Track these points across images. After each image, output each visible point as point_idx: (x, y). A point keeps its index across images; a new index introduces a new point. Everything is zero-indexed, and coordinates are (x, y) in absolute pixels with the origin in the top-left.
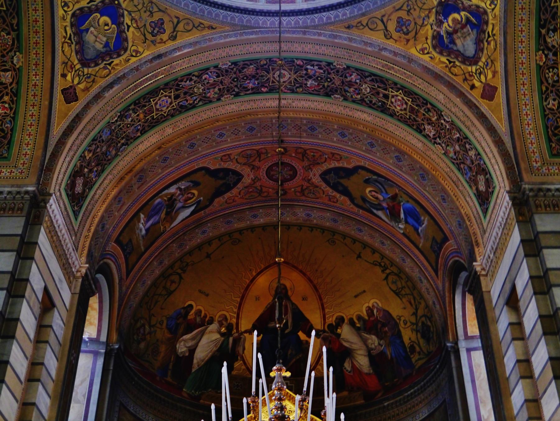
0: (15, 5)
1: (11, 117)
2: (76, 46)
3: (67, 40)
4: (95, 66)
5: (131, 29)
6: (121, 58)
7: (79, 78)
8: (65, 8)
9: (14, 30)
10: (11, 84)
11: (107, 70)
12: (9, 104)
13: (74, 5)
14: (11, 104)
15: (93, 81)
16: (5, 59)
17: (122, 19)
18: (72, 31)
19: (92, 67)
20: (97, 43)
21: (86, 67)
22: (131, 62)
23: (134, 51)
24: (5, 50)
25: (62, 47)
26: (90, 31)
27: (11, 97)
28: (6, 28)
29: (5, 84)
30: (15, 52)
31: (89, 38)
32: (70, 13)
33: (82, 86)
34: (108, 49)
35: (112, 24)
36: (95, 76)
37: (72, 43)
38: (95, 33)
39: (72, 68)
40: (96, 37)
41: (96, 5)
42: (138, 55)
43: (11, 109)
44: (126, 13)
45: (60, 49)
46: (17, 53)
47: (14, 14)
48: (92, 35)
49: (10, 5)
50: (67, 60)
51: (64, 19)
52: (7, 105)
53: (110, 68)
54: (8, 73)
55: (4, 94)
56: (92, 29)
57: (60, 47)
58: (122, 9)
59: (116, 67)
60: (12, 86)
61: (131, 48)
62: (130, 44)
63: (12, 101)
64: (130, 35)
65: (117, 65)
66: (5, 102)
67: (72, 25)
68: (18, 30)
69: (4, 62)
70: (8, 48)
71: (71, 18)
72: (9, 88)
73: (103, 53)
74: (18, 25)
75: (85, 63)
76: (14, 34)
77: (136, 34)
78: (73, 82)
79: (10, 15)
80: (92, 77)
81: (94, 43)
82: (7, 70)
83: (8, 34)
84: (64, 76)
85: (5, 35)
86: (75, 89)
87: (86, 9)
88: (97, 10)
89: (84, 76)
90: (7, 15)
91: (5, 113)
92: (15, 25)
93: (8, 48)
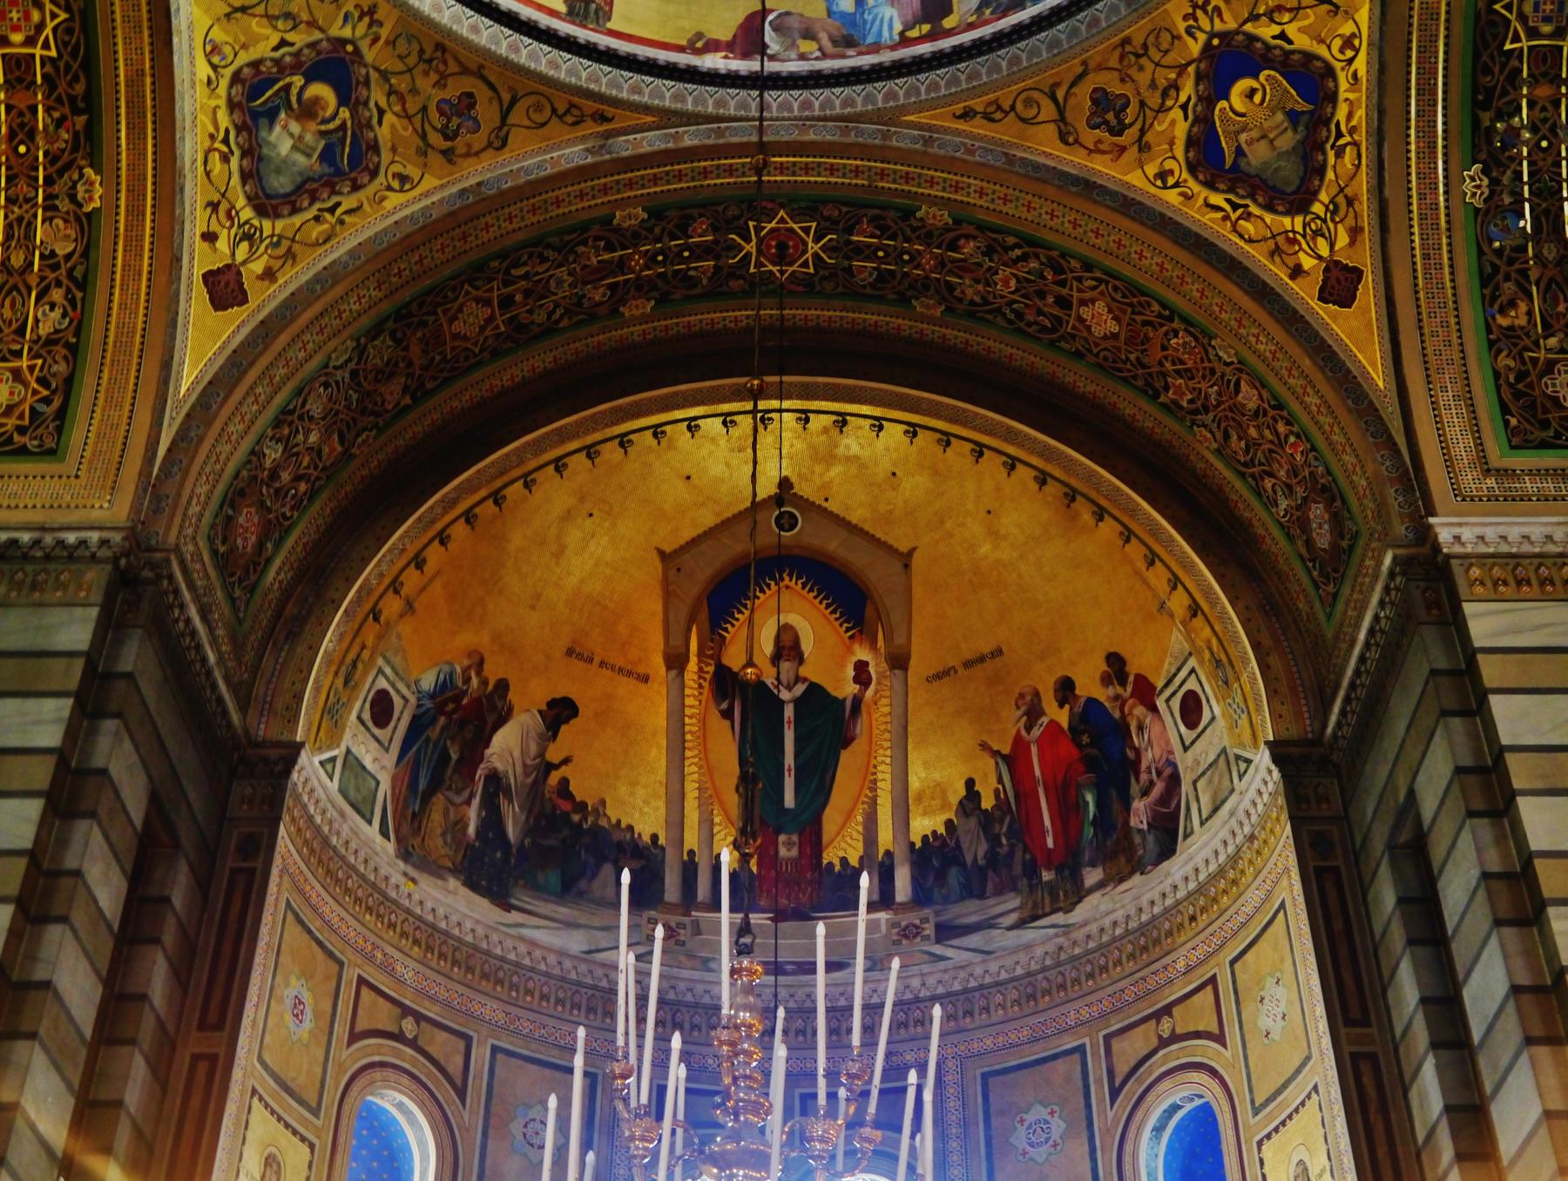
2: (1255, 201)
3: (1234, 217)
4: (1322, 180)
5: (1291, 31)
6: (1342, 95)
7: (1323, 235)
8: (1171, 181)
11: (1348, 149)
12: (1291, 432)
13: (1174, 158)
15: (1350, 202)
17: (1259, 45)
18: (1223, 192)
19: (1320, 187)
20: (1277, 143)
21: (1311, 203)
22: (1362, 73)
23: (1342, 51)
25: (1241, 237)
26: (1244, 146)
31: (1258, 155)
32: (1185, 175)
33: (1343, 240)
34: (1305, 119)
35: (1256, 77)
36: (1342, 190)
37: (1246, 206)
38: (1255, 134)
39: (1294, 241)
40: (1264, 137)
41: (1200, 99)
42: (1356, 42)
44: (1248, 27)
45: (1242, 243)
48: (1256, 145)
49: (1124, 296)
50: (1271, 244)
51: (1187, 197)
52: (1292, 439)
53: (1348, 139)
56: (1243, 137)
57: (1238, 241)
58: (1237, 32)
59: (1354, 123)
61: (1331, 53)
62: (1322, 51)
63: (1288, 423)
64: (1302, 42)
65: (1350, 116)
66: (1287, 437)
67: (1210, 185)
68: (1172, 312)
71: (1196, 178)
73: (1306, 137)
75: (1299, 202)
77: (1306, 23)
78: (1320, 257)
80: (1341, 199)
81: (1274, 148)
82: (1238, 384)
84: (1297, 272)
86: (1337, 263)
87: (1195, 130)
88: (1209, 101)
89: (1324, 221)
90: (1140, 313)
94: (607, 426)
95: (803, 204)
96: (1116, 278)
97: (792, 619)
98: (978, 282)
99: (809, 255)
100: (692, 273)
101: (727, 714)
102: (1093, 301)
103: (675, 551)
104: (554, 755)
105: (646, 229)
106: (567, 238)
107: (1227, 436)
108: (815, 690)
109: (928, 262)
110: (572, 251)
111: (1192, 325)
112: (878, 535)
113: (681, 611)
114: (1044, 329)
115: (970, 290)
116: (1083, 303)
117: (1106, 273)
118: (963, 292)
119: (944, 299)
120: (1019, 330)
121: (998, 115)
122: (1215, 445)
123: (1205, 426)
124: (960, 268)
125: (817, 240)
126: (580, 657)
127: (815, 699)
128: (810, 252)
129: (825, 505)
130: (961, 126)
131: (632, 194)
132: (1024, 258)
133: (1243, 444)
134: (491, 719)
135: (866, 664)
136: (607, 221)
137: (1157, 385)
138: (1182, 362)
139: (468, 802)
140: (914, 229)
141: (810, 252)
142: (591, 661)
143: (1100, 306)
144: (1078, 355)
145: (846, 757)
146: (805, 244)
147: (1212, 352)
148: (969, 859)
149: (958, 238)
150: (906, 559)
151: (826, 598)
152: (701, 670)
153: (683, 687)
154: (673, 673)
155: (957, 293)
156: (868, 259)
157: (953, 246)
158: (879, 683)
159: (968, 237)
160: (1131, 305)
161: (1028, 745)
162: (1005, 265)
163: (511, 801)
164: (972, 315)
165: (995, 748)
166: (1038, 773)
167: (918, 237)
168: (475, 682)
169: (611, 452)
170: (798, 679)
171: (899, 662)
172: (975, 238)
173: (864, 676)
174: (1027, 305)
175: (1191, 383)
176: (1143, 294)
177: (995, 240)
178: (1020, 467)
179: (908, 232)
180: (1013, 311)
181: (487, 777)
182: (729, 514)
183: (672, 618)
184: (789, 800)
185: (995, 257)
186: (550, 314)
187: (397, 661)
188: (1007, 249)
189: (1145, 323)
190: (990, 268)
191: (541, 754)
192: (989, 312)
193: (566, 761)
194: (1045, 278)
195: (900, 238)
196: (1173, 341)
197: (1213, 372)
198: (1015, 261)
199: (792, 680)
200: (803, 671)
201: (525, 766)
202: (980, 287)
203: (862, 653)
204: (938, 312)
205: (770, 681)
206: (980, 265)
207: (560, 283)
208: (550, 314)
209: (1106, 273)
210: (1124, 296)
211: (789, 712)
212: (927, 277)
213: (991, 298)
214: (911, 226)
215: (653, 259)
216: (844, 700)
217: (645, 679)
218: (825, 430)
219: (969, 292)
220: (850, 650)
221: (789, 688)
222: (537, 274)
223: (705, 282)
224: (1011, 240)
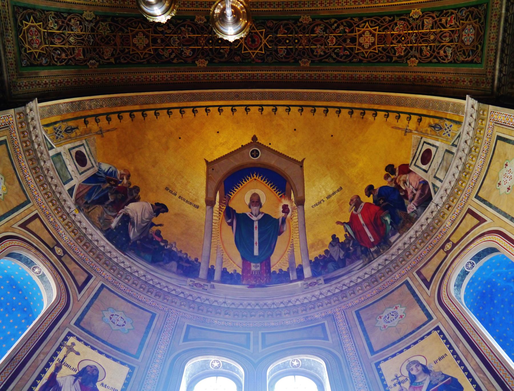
0: (375, 19)
1: (458, 12)
9: (394, 19)
10: (433, 18)
12: (448, 17)
14: (448, 14)
16: (414, 26)
24: (408, 27)
27: (443, 16)
28: (391, 26)
29: (433, 24)
30: (410, 17)
43: (452, 13)
46: (411, 15)
47: (382, 19)
49: (375, 22)
54: (425, 23)
55: (440, 24)
60: (435, 17)
68: (393, 16)
69: (416, 27)
70: (406, 25)
72: (436, 19)
74: (390, 16)
76: (397, 19)
79: (383, 23)
82: (423, 23)
85: (397, 27)
90: (382, 26)
91: (454, 19)
92: (390, 19)
93: (406, 25)
94: (188, 101)
95: (260, 21)
97: (258, 191)
98: (321, 45)
99: (262, 45)
100: (222, 51)
101: (231, 224)
102: (364, 33)
103: (212, 162)
104: (155, 220)
105: (206, 26)
106: (178, 22)
107: (421, 51)
108: (267, 217)
109: (304, 41)
110: (179, 28)
111: (402, 15)
112: (290, 156)
113: (214, 185)
114: (348, 56)
115: (319, 49)
116: (360, 36)
118: (317, 52)
119: (310, 57)
120: (338, 62)
122: (417, 61)
123: (412, 57)
124: (315, 41)
125: (265, 37)
126: (171, 192)
127: (266, 220)
128: (263, 43)
129: (269, 146)
131: (201, 9)
132: (338, 27)
133: (429, 48)
134: (130, 198)
135: (287, 205)
136: (193, 19)
137: (392, 55)
139: (114, 217)
140: (299, 27)
141: (263, 43)
142: (175, 195)
143: (367, 34)
144: (361, 61)
145: (279, 238)
146: (261, 39)
147: (410, 20)
148: (336, 259)
149: (314, 27)
150: (301, 164)
151: (270, 183)
152: (220, 207)
153: (213, 212)
154: (209, 207)
155: (315, 53)
156: (283, 45)
157: (313, 32)
158: (293, 212)
159: (317, 25)
161: (357, 215)
162: (332, 33)
163: (133, 226)
164: (320, 62)
165: (343, 221)
166: (362, 222)
167: (300, 31)
168: (125, 181)
169: (189, 112)
170: (259, 213)
171: (301, 202)
172: (320, 25)
173: (286, 210)
174: (340, 48)
175: (404, 42)
176: (382, 16)
177: (327, 23)
178: (343, 111)
179: (296, 28)
180: (336, 53)
181: (124, 215)
182: (233, 150)
183: (209, 187)
184: (256, 252)
185: (328, 31)
186: (171, 54)
187: (92, 149)
188: (331, 25)
190: (326, 36)
191: (150, 219)
192: (326, 58)
193: (161, 225)
194: (345, 32)
195: (294, 32)
198: (335, 30)
199: (257, 214)
200: (262, 210)
201: (142, 220)
202: (323, 47)
203: (285, 202)
204: (308, 65)
205: (248, 214)
206: (322, 37)
207: (175, 41)
208: (171, 54)
211: (256, 224)
212: (304, 49)
213: (327, 52)
214: (297, 26)
215: (208, 41)
216: (278, 219)
217: (198, 207)
218: (269, 114)
219: (319, 51)
220: (280, 201)
221: (256, 216)
222: (166, 33)
223: (226, 56)
224: (333, 20)
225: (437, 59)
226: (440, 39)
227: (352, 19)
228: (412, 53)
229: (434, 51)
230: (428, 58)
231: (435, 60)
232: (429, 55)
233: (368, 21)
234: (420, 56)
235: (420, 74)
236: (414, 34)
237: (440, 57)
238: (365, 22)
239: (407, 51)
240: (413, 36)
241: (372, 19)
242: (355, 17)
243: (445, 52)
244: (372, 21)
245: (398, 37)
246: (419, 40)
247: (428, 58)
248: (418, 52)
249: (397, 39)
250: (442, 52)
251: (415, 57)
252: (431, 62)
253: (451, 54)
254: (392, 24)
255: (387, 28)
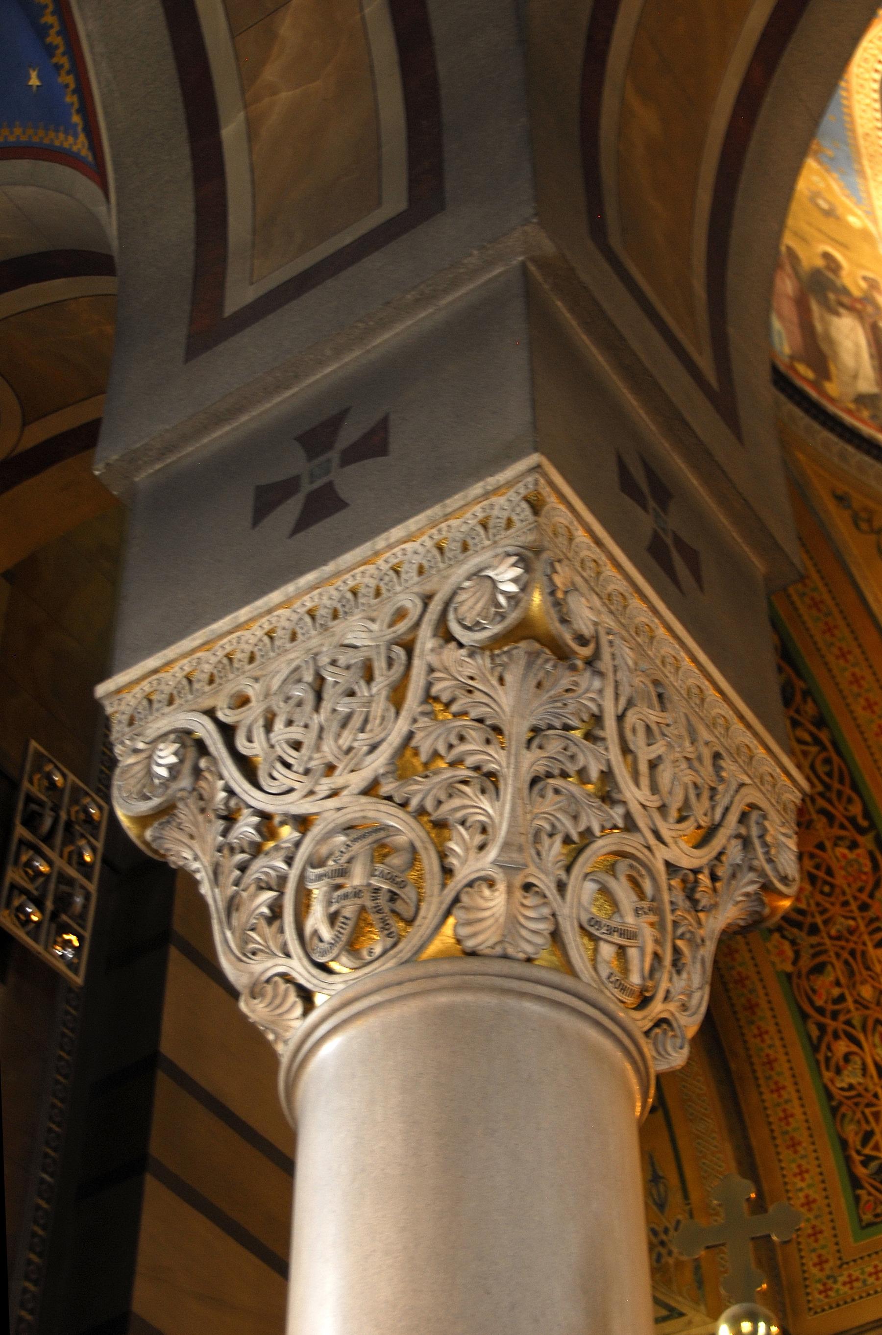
9: (862, 831)
24: (861, 890)
28: (843, 833)
47: (848, 791)
49: (829, 774)
68: (873, 826)
69: (872, 921)
74: (867, 814)
83: (853, 846)
85: (846, 851)
90: (830, 801)
96: (839, 753)
107: (819, 969)
117: (834, 744)
121: (864, 526)
122: (789, 968)
123: (793, 943)
130: (831, 506)
133: (836, 992)
138: (829, 872)
160: (828, 787)
175: (819, 898)
176: (855, 787)
189: (823, 812)
196: (841, 850)
197: (864, 907)
209: (834, 744)
210: (829, 774)
225: (820, 1039)
226: (870, 1023)
227: (806, 694)
228: (806, 940)
229: (835, 1016)
230: (811, 1002)
231: (815, 1032)
232: (819, 1003)
233: (824, 748)
234: (804, 971)
235: (761, 992)
236: (852, 923)
237: (829, 1048)
238: (817, 741)
239: (800, 918)
240: (846, 918)
241: (835, 758)
242: (815, 701)
243: (847, 1058)
244: (828, 761)
245: (824, 868)
246: (843, 948)
247: (811, 1002)
248: (815, 955)
249: (818, 867)
250: (842, 1047)
251: (797, 954)
252: (805, 1016)
253: (851, 1087)
254: (850, 833)
255: (830, 818)
